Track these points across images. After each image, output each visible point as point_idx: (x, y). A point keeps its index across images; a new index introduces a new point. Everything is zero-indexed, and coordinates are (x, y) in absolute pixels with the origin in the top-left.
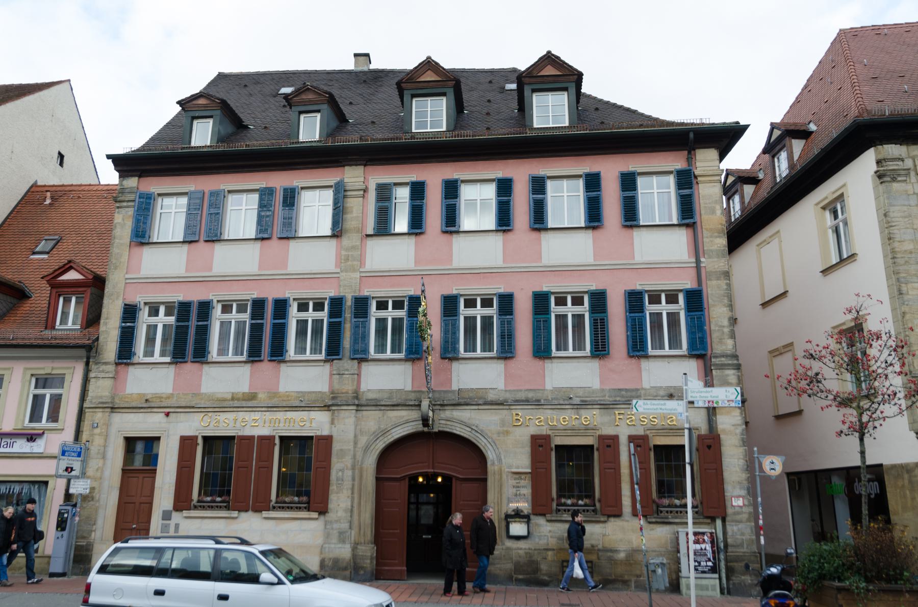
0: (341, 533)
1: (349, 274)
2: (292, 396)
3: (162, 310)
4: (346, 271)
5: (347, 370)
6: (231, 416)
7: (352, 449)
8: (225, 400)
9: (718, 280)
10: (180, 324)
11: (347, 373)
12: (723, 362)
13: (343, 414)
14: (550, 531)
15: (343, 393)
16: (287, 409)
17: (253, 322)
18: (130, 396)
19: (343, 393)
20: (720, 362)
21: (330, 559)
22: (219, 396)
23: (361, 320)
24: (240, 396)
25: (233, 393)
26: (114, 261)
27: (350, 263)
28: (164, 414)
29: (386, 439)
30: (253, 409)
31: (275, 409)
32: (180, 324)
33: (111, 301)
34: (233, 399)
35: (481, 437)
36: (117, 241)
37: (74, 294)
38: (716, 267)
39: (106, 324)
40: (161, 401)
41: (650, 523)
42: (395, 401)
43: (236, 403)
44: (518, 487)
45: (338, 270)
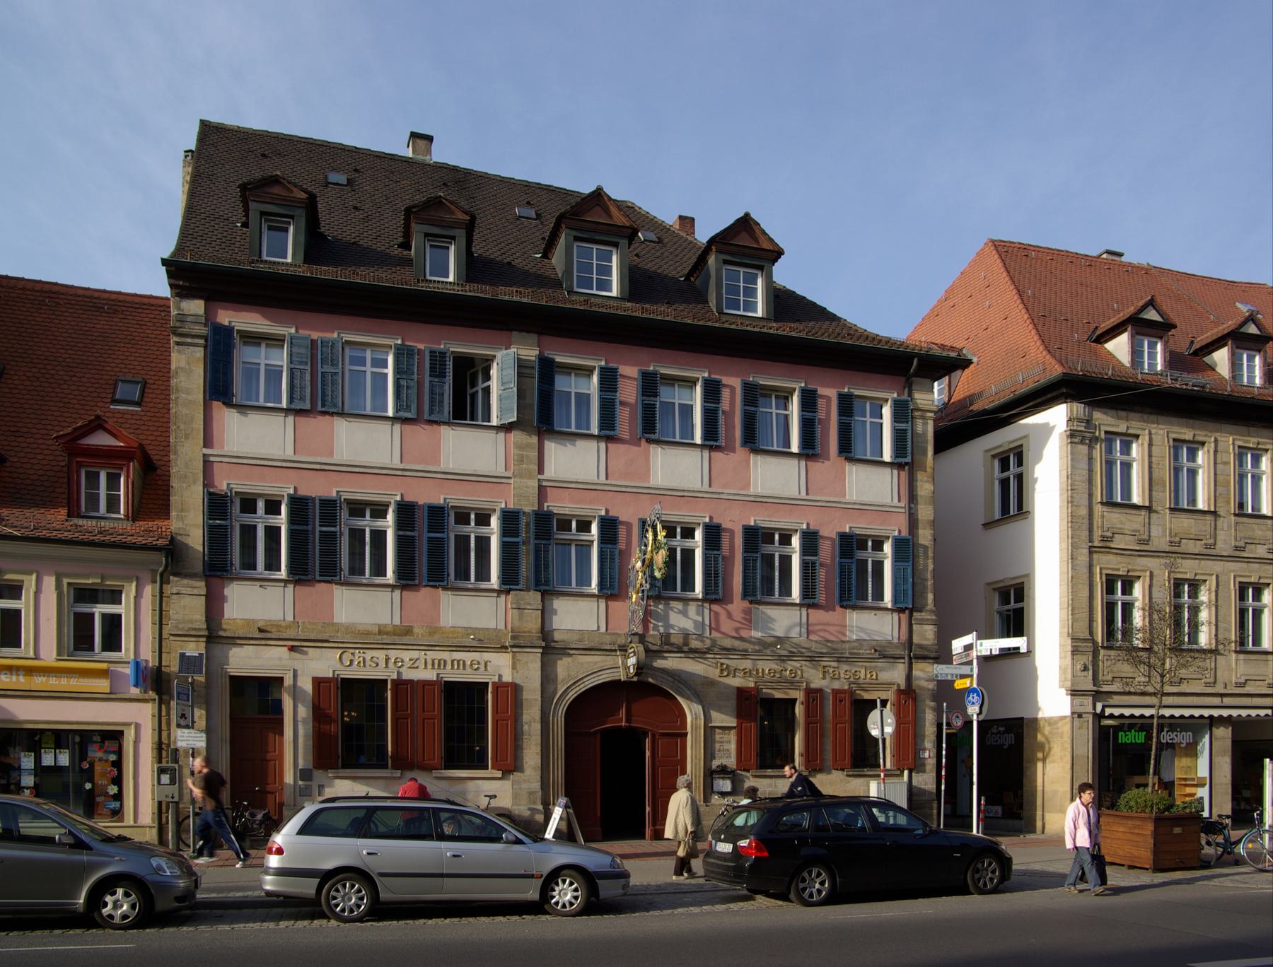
1: (524, 481)
2: (458, 633)
3: (261, 505)
4: (521, 477)
6: (381, 655)
7: (540, 699)
8: (368, 633)
11: (529, 607)
15: (525, 632)
16: (454, 649)
17: (401, 533)
18: (232, 622)
22: (361, 628)
23: (544, 542)
24: (390, 629)
25: (379, 626)
28: (286, 648)
29: (577, 689)
30: (408, 647)
31: (437, 648)
32: (296, 527)
34: (380, 633)
35: (684, 688)
36: (183, 395)
40: (279, 631)
42: (586, 644)
43: (387, 639)
45: (509, 474)
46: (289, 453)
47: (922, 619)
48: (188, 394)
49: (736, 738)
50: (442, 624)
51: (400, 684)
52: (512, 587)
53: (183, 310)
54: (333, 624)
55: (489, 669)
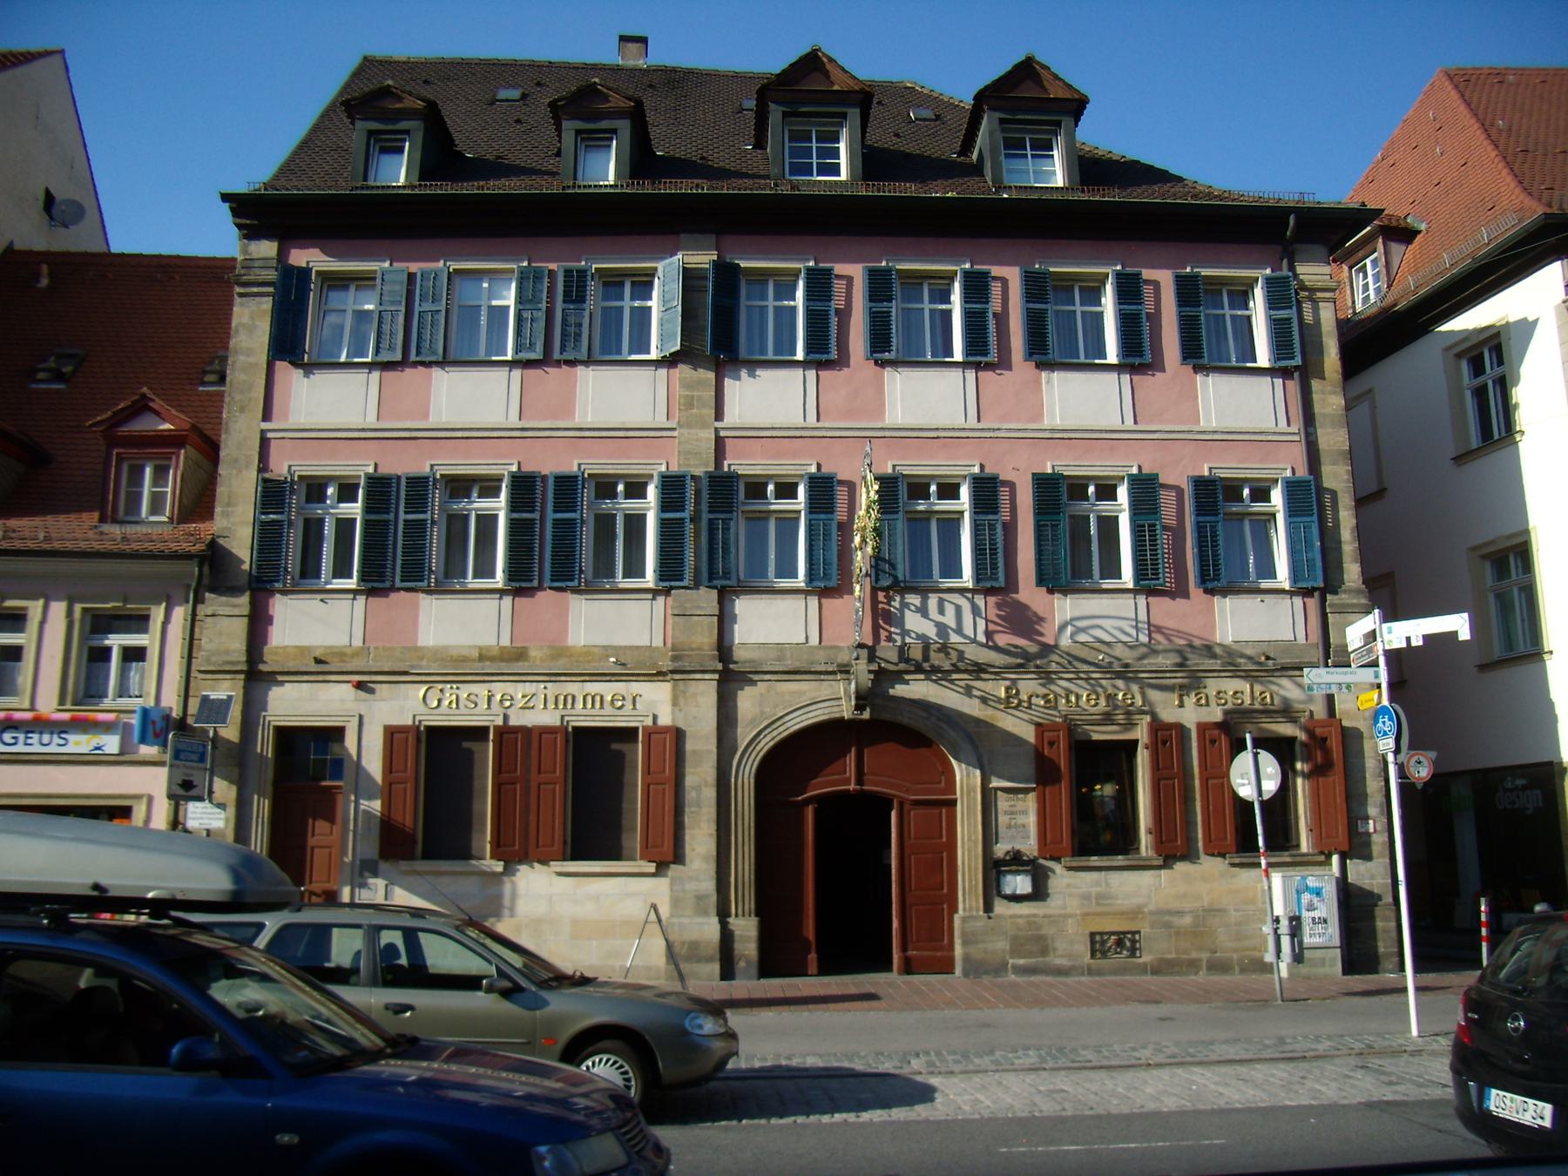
0: (700, 898)
1: (693, 431)
4: (689, 426)
5: (699, 608)
6: (481, 690)
7: (715, 750)
8: (465, 660)
9: (1334, 464)
10: (373, 517)
12: (1344, 601)
13: (694, 687)
14: (1068, 886)
15: (692, 650)
16: (587, 678)
17: (516, 516)
18: (281, 651)
19: (692, 650)
20: (1340, 602)
21: (683, 943)
22: (454, 653)
23: (722, 516)
24: (495, 652)
25: (480, 648)
26: (238, 397)
27: (694, 411)
29: (775, 733)
31: (563, 678)
32: (373, 517)
33: (235, 472)
34: (482, 658)
37: (149, 459)
38: (1332, 442)
39: (226, 515)
41: (1233, 865)
42: (789, 664)
43: (489, 667)
44: (1012, 813)
46: (371, 420)
47: (1344, 605)
48: (248, 355)
49: (1036, 805)
50: (419, 645)
51: (506, 733)
52: (673, 584)
53: (251, 254)
54: (417, 649)
55: (638, 706)
